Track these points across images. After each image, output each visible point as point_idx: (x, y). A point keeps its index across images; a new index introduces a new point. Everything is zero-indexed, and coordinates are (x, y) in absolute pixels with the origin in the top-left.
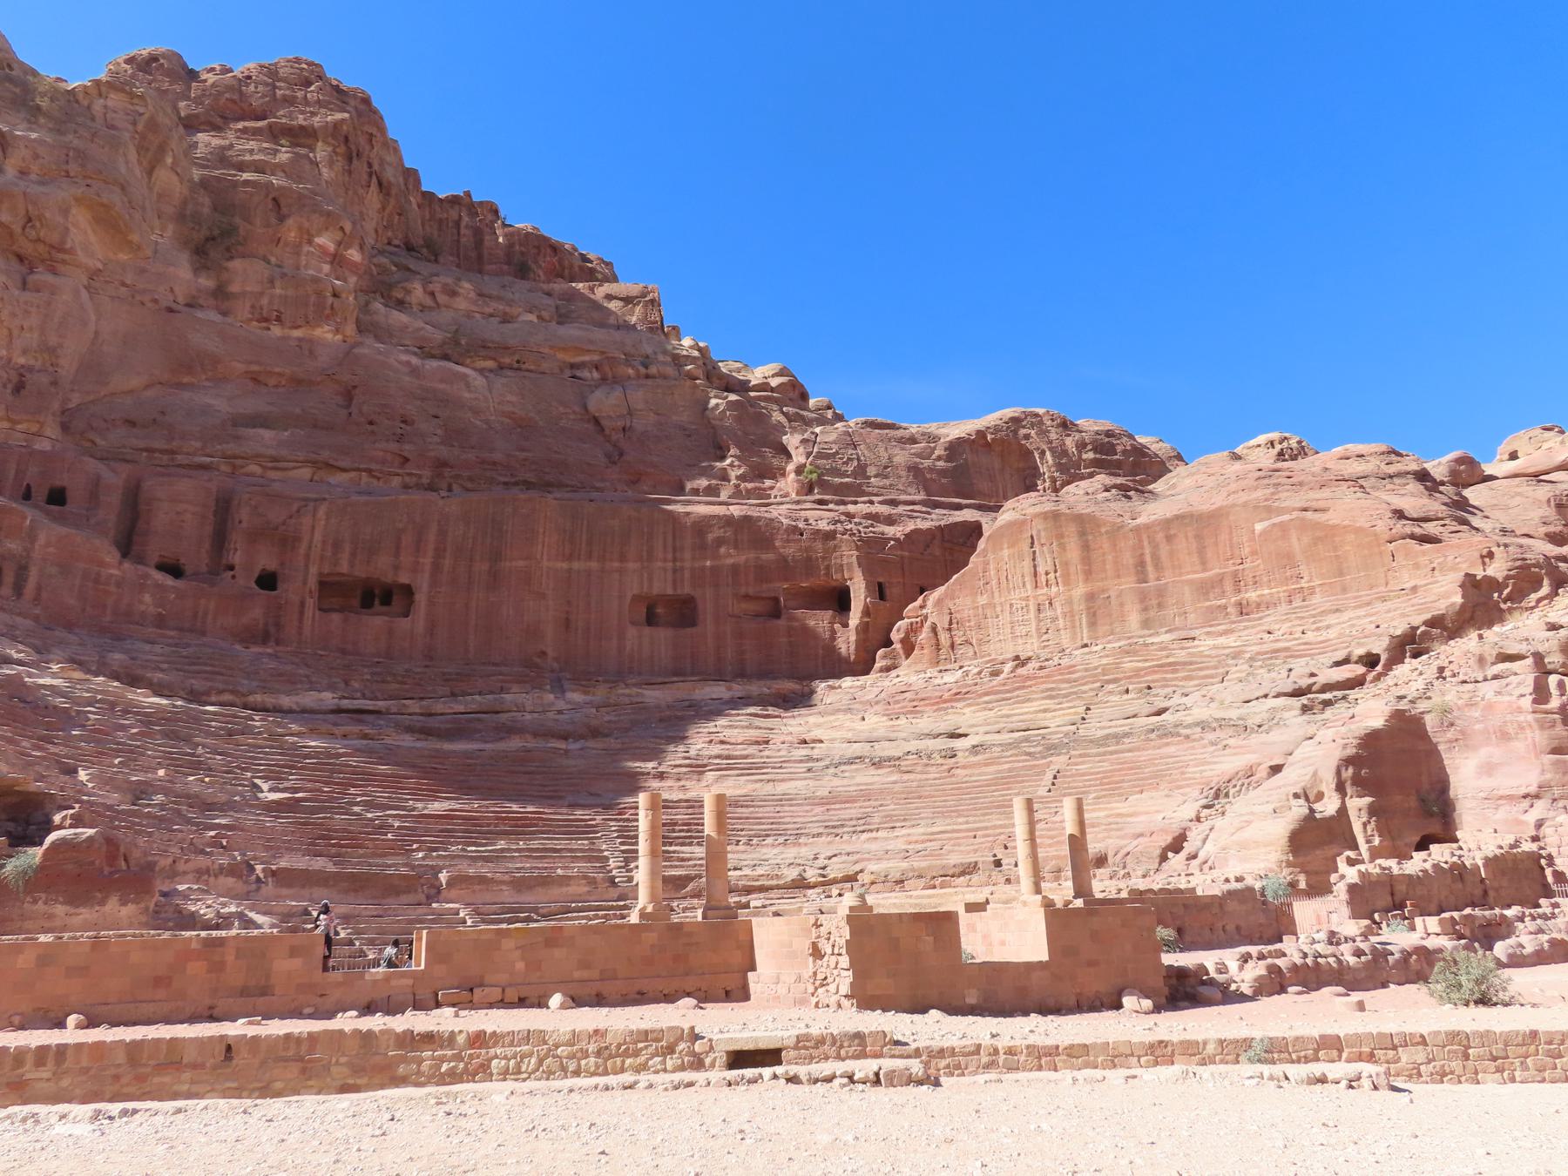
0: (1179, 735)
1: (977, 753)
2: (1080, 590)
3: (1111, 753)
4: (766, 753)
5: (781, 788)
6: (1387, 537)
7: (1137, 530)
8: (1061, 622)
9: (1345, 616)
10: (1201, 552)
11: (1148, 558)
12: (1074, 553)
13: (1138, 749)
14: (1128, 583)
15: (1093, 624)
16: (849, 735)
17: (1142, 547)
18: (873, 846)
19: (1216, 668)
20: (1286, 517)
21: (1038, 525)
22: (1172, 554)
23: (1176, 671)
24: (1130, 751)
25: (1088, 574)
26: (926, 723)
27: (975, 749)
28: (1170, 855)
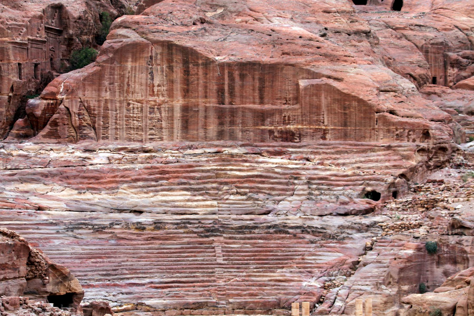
0: (287, 233)
2: (178, 103)
3: (249, 239)
6: (375, 109)
7: (222, 66)
10: (261, 90)
11: (226, 88)
12: (178, 75)
14: (212, 102)
15: (186, 126)
17: (223, 79)
19: (287, 184)
21: (157, 50)
22: (242, 86)
23: (263, 182)
25: (186, 92)
27: (158, 225)
28: (317, 305)
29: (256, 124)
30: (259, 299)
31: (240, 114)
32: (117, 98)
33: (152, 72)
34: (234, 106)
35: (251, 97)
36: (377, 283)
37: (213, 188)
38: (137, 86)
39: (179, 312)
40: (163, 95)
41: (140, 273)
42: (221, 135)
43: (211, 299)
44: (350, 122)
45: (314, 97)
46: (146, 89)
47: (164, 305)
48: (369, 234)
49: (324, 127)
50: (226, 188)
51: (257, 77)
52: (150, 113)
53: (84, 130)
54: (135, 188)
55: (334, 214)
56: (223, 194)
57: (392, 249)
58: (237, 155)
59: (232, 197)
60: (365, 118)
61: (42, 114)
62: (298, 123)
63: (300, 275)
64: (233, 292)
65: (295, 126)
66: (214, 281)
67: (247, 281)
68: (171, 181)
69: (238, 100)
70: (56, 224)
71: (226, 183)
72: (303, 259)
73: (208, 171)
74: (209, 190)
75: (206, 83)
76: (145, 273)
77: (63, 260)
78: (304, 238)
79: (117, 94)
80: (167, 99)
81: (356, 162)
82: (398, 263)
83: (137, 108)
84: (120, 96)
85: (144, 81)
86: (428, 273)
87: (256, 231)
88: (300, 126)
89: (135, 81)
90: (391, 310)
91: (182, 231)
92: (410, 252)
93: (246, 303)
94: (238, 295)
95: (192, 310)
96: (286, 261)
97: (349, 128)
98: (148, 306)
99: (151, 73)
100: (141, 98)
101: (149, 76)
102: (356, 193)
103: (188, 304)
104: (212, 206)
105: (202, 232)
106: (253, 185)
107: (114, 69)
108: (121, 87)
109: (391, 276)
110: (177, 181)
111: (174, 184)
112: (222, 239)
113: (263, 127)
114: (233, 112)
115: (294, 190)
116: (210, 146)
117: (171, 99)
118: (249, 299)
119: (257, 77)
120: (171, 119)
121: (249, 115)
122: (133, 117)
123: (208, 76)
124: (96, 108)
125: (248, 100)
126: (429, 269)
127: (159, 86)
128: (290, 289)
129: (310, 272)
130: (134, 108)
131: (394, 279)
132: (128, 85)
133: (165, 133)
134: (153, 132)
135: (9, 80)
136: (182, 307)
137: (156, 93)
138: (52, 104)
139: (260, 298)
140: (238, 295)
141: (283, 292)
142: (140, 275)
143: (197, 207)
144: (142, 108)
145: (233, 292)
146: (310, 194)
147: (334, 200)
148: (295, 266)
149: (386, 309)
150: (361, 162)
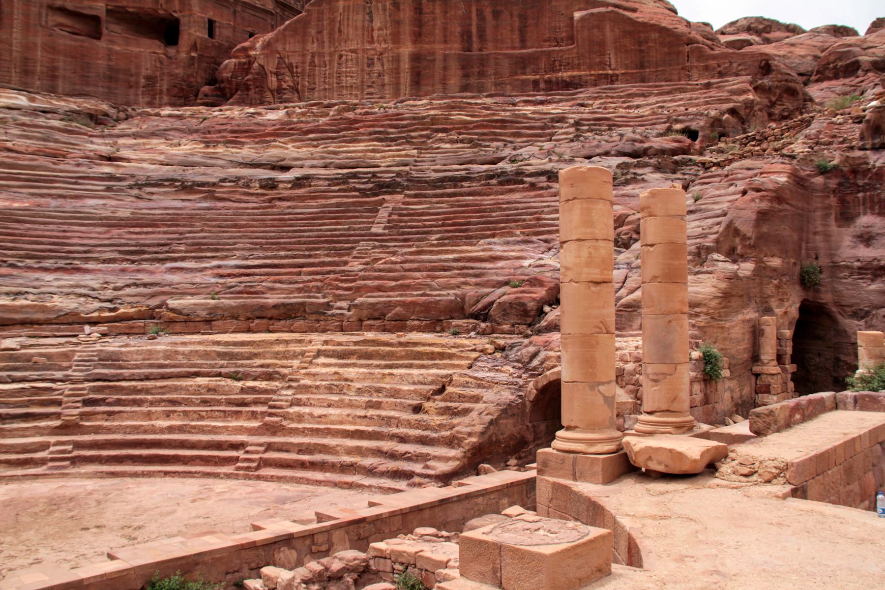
1: (301, 186)
2: (407, 50)
4: (62, 167)
5: (70, 205)
8: (386, 79)
9: (652, 100)
10: (522, 31)
11: (474, 30)
13: (479, 194)
14: (455, 48)
16: (162, 158)
17: (470, 18)
18: (176, 278)
20: (602, 10)
22: (497, 27)
23: (505, 128)
24: (469, 194)
25: (418, 37)
26: (247, 152)
28: (547, 309)
29: (513, 73)
30: (418, 295)
31: (492, 62)
32: (326, 50)
33: (371, 12)
34: (485, 52)
35: (509, 41)
36: (698, 248)
37: (421, 136)
38: (351, 31)
39: (244, 325)
40: (385, 41)
41: (208, 250)
42: (465, 88)
43: (318, 298)
44: (649, 62)
45: (595, 31)
46: (363, 35)
47: (211, 309)
48: (679, 175)
49: (610, 72)
50: (440, 135)
51: (515, 13)
52: (369, 66)
53: (285, 94)
54: (303, 141)
55: (613, 152)
56: (432, 143)
57: (732, 185)
58: (476, 104)
59: (448, 146)
60: (669, 54)
61: (232, 77)
62: (573, 69)
63: (523, 247)
64: (369, 283)
65: (569, 73)
66: (346, 263)
67: (411, 261)
68: (361, 130)
69: (490, 45)
70: (120, 179)
71: (444, 131)
72: (538, 219)
73: (424, 118)
74: (414, 138)
75: (446, 23)
76: (217, 250)
77: (65, 227)
78: (551, 188)
79: (327, 44)
80: (391, 46)
81: (657, 102)
82: (753, 200)
83: (352, 60)
84: (330, 47)
85: (359, 24)
86: (818, 238)
87: (465, 184)
88: (575, 73)
89: (348, 25)
90: (740, 317)
91: (337, 188)
92: (783, 179)
93: (389, 305)
94: (379, 289)
95: (271, 322)
96: (503, 225)
97: (648, 70)
98: (173, 310)
99: (370, 14)
100: (356, 47)
101: (367, 17)
102: (655, 132)
103: (263, 307)
104: (407, 156)
105: (370, 189)
106: (485, 131)
107: (322, 13)
108: (331, 34)
109: (737, 232)
110: (371, 129)
111: (363, 134)
112: (399, 197)
113: (524, 77)
114: (483, 61)
115: (553, 134)
116: (442, 98)
117: (396, 46)
118: (395, 296)
119: (515, 13)
120: (397, 71)
121: (506, 63)
122: (346, 72)
123: (448, 15)
124: (300, 65)
125: (504, 46)
126: (820, 229)
127: (380, 29)
128: (492, 274)
129: (546, 241)
130: (347, 61)
131: (744, 238)
132: (340, 31)
133: (388, 90)
134: (371, 90)
135: (190, 34)
136: (249, 315)
137: (375, 38)
138: (245, 64)
139: (422, 295)
140: (379, 289)
141: (474, 280)
142: (209, 254)
143: (384, 157)
144: (357, 59)
145: (369, 283)
146: (576, 136)
147: (618, 138)
148: (518, 232)
149: (726, 315)
150: (665, 101)
